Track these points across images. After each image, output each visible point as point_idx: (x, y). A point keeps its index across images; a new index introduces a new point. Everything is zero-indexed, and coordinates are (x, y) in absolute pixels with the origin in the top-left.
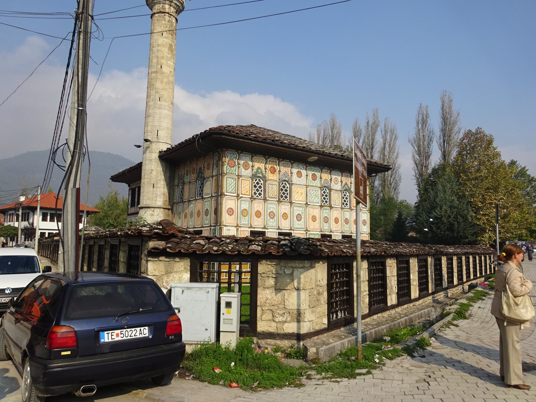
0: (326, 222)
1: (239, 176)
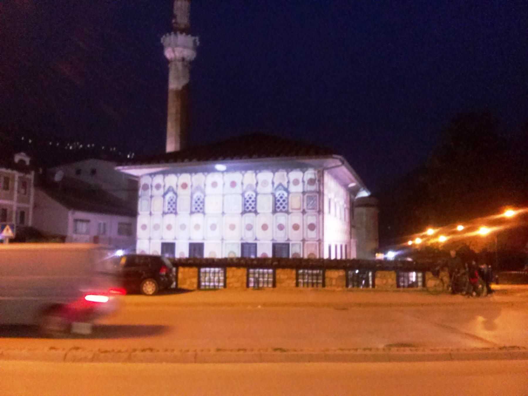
1: (151, 197)
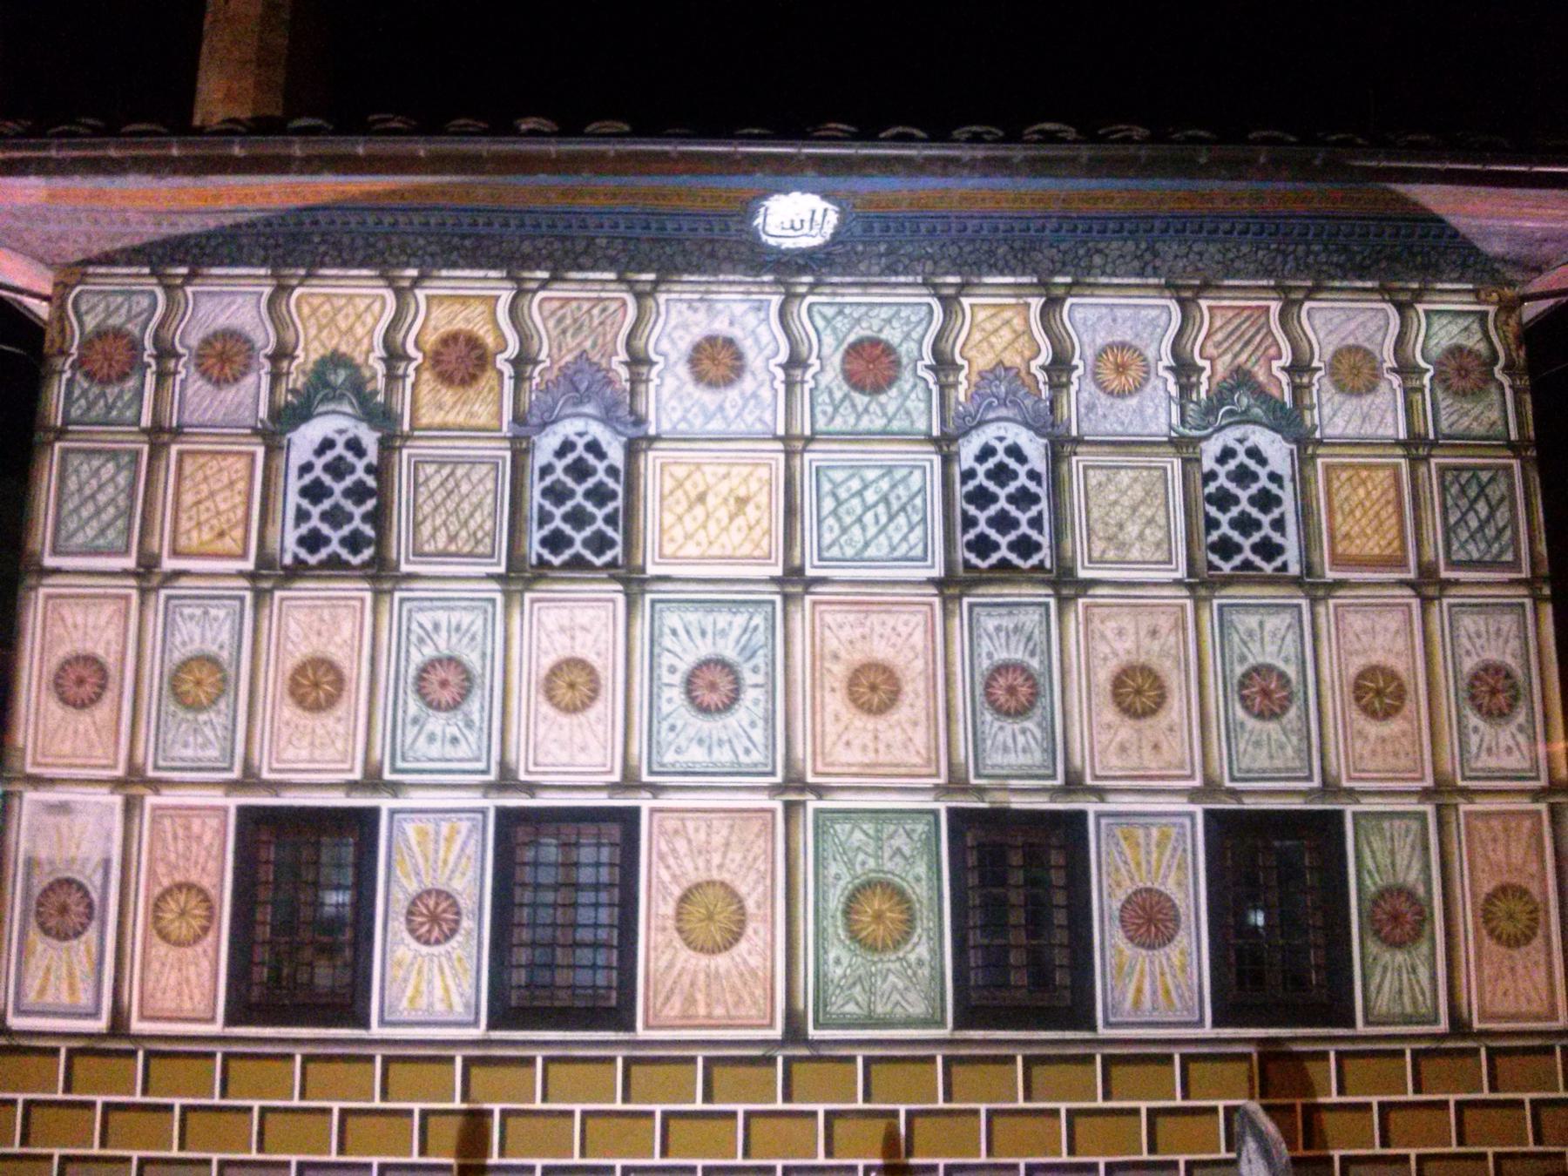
0: (1021, 712)
1: (160, 434)
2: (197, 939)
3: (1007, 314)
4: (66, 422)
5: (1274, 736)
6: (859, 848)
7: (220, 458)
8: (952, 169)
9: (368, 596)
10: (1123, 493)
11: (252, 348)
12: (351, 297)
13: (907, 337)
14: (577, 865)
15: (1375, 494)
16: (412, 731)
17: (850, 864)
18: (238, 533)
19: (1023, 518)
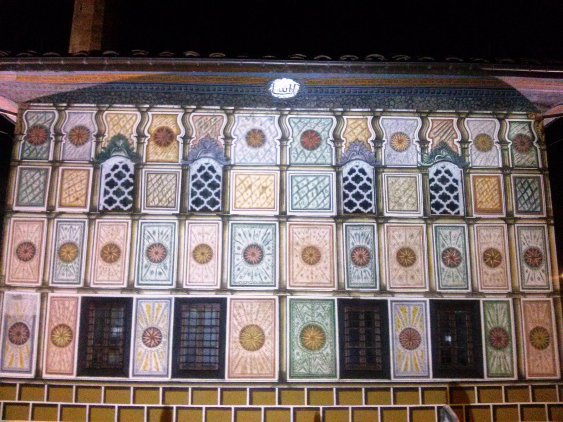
0: (364, 264)
1: (56, 163)
2: (67, 345)
3: (360, 122)
4: (22, 159)
5: (455, 273)
6: (306, 313)
7: (77, 172)
8: (340, 70)
9: (130, 221)
10: (401, 186)
11: (89, 133)
12: (125, 115)
13: (324, 130)
14: (204, 319)
15: (491, 187)
16: (145, 270)
17: (303, 319)
18: (83, 198)
19: (365, 195)
